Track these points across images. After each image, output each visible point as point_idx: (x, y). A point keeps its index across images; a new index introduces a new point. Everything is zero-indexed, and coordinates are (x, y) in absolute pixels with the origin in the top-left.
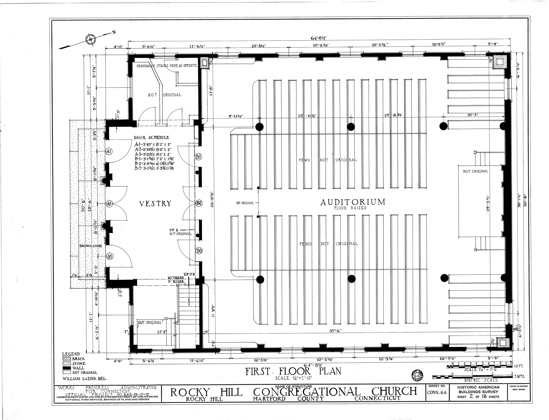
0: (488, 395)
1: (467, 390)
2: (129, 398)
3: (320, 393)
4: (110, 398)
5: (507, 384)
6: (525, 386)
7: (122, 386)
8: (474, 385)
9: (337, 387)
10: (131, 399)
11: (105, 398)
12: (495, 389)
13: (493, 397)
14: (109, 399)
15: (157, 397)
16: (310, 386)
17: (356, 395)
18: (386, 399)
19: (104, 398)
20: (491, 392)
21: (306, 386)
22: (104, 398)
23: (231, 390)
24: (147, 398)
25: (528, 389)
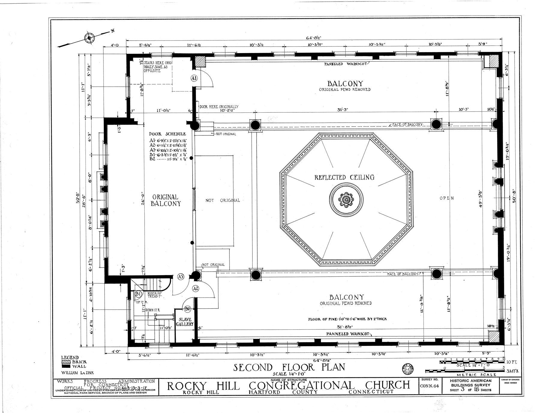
0: (480, 388)
1: (460, 383)
2: (127, 391)
3: (314, 387)
4: (108, 392)
5: (499, 377)
6: (516, 380)
7: (119, 380)
9: (331, 380)
10: (129, 393)
11: (103, 391)
12: (488, 383)
13: (485, 390)
15: (154, 390)
16: (305, 379)
17: (350, 388)
18: (379, 392)
19: (102, 391)
21: (301, 380)
22: (102, 391)
23: (228, 384)
24: (144, 391)
25: (519, 382)
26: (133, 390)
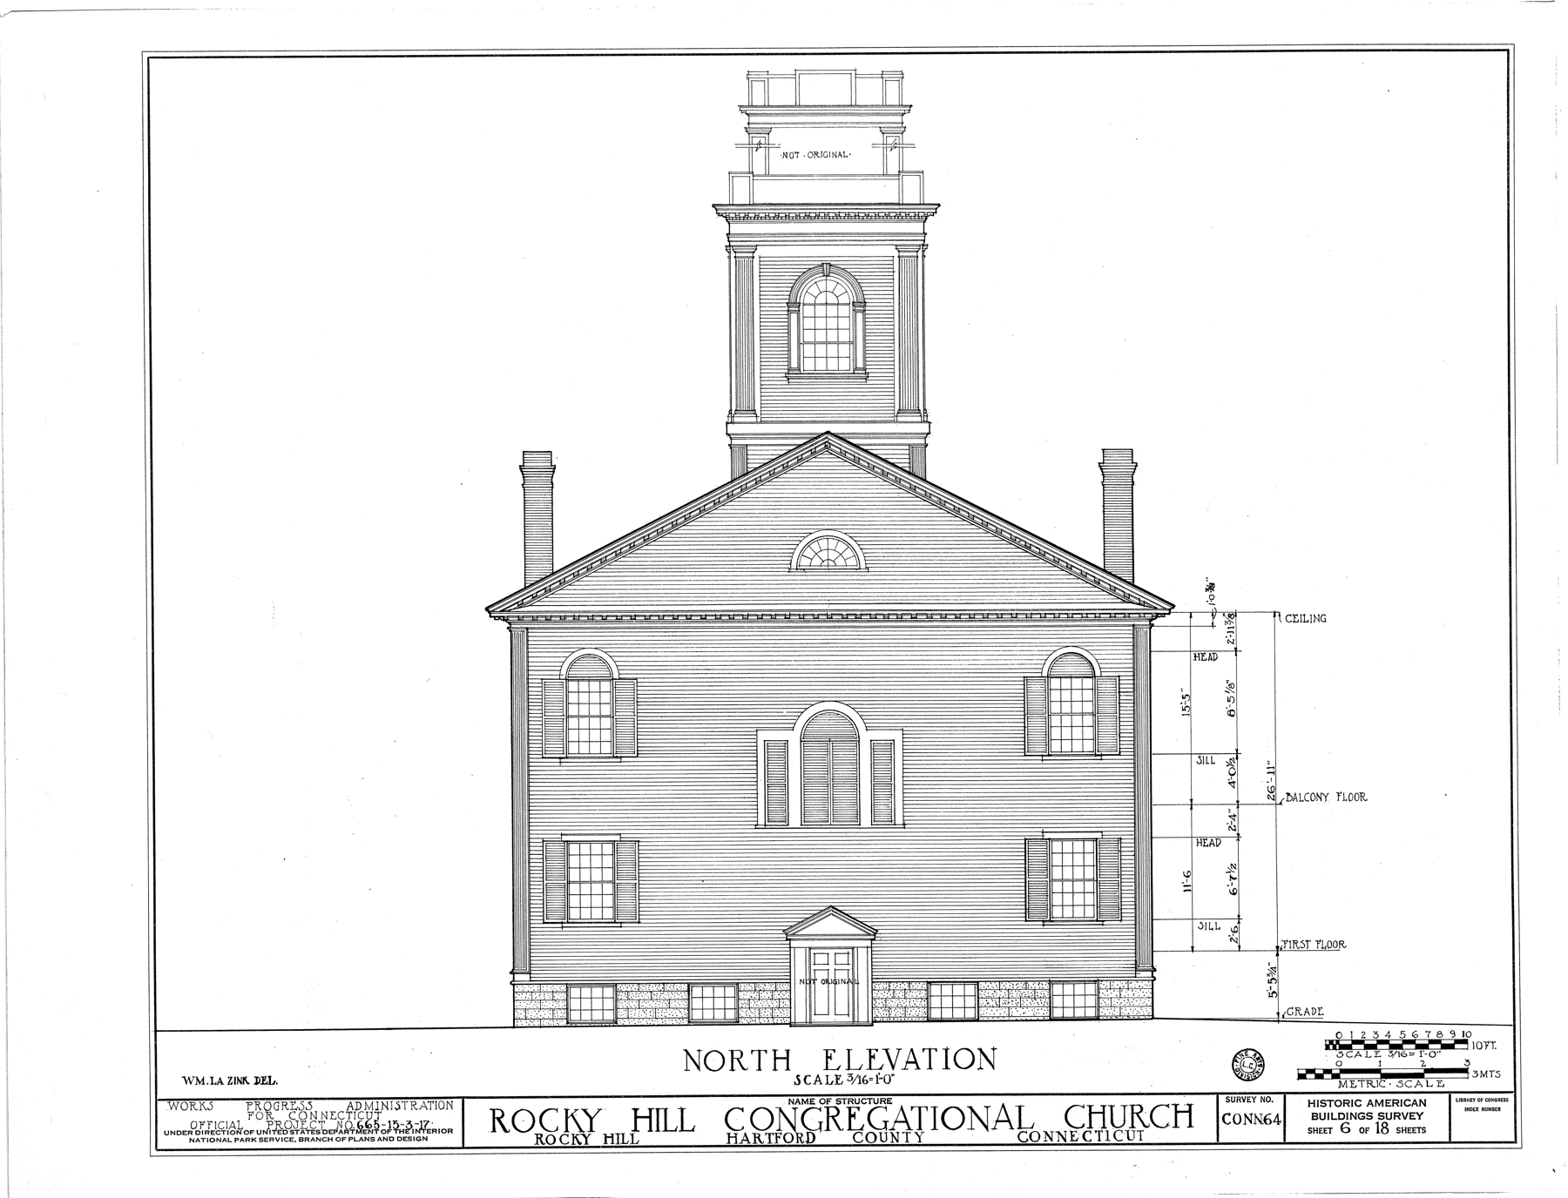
1: (1335, 1110)
2: (370, 1135)
3: (914, 1124)
4: (315, 1136)
6: (1500, 1100)
8: (1354, 1097)
9: (963, 1103)
10: (376, 1139)
11: (303, 1135)
12: (1414, 1109)
13: (1407, 1130)
14: (313, 1139)
15: (450, 1131)
16: (886, 1099)
17: (1020, 1128)
19: (300, 1135)
20: (1401, 1117)
21: (876, 1101)
22: (300, 1135)
24: (422, 1135)
26: (389, 1131)
